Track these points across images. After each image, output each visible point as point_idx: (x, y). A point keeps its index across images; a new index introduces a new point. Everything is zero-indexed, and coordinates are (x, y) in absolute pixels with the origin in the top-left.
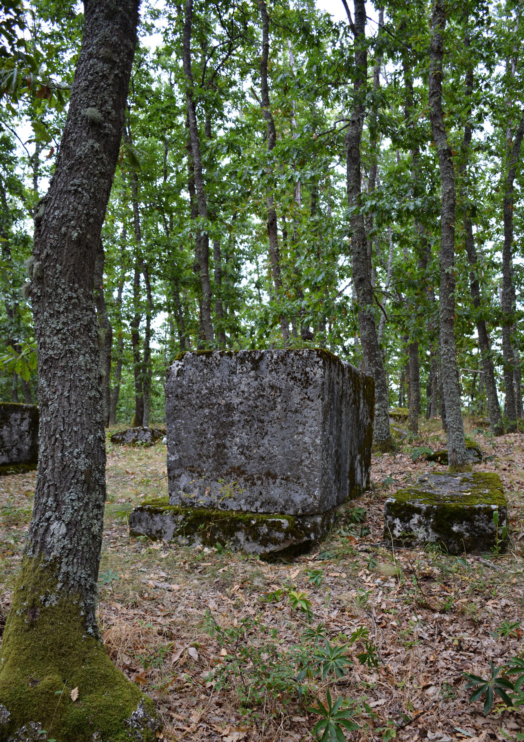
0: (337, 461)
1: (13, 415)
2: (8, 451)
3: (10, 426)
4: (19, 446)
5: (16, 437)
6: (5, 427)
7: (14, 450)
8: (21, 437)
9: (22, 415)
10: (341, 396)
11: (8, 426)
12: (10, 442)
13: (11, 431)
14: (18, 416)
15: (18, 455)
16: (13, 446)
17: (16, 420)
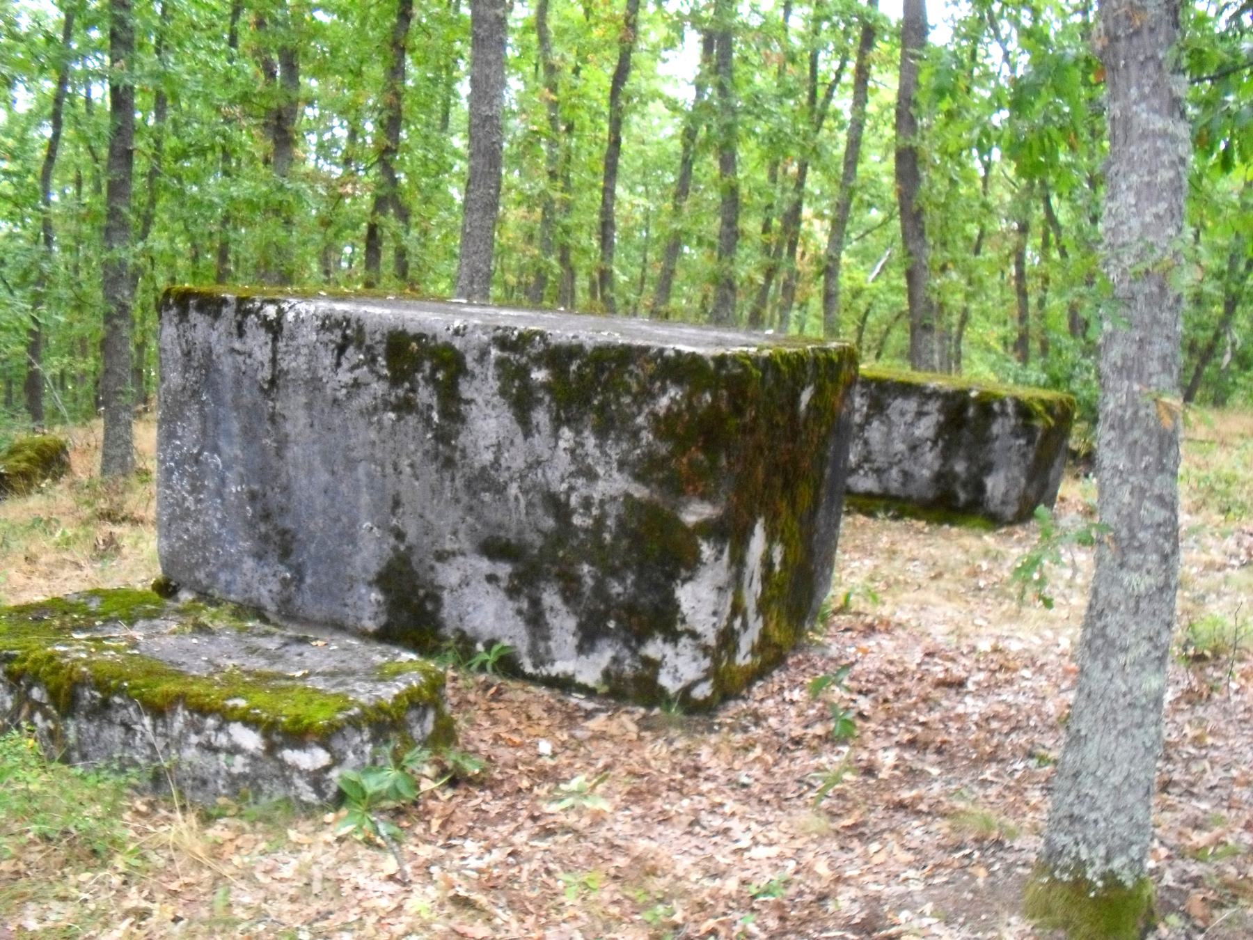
0: (266, 516)
1: (898, 403)
2: (879, 472)
3: (890, 424)
4: (907, 465)
5: (900, 447)
6: (875, 424)
7: (894, 472)
8: (913, 449)
9: (921, 404)
10: (273, 382)
11: (882, 422)
12: (886, 453)
13: (889, 433)
14: (911, 405)
15: (904, 484)
16: (891, 465)
17: (902, 414)
